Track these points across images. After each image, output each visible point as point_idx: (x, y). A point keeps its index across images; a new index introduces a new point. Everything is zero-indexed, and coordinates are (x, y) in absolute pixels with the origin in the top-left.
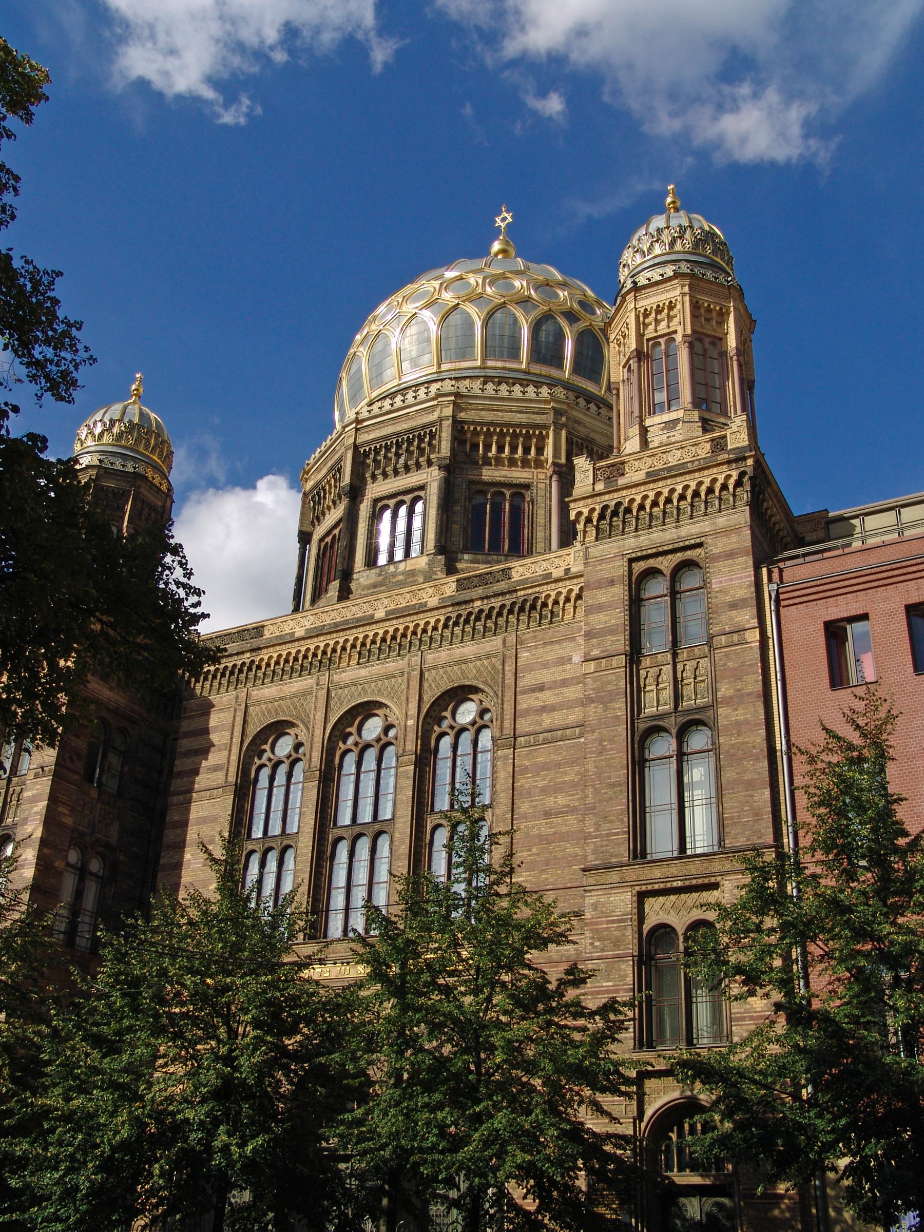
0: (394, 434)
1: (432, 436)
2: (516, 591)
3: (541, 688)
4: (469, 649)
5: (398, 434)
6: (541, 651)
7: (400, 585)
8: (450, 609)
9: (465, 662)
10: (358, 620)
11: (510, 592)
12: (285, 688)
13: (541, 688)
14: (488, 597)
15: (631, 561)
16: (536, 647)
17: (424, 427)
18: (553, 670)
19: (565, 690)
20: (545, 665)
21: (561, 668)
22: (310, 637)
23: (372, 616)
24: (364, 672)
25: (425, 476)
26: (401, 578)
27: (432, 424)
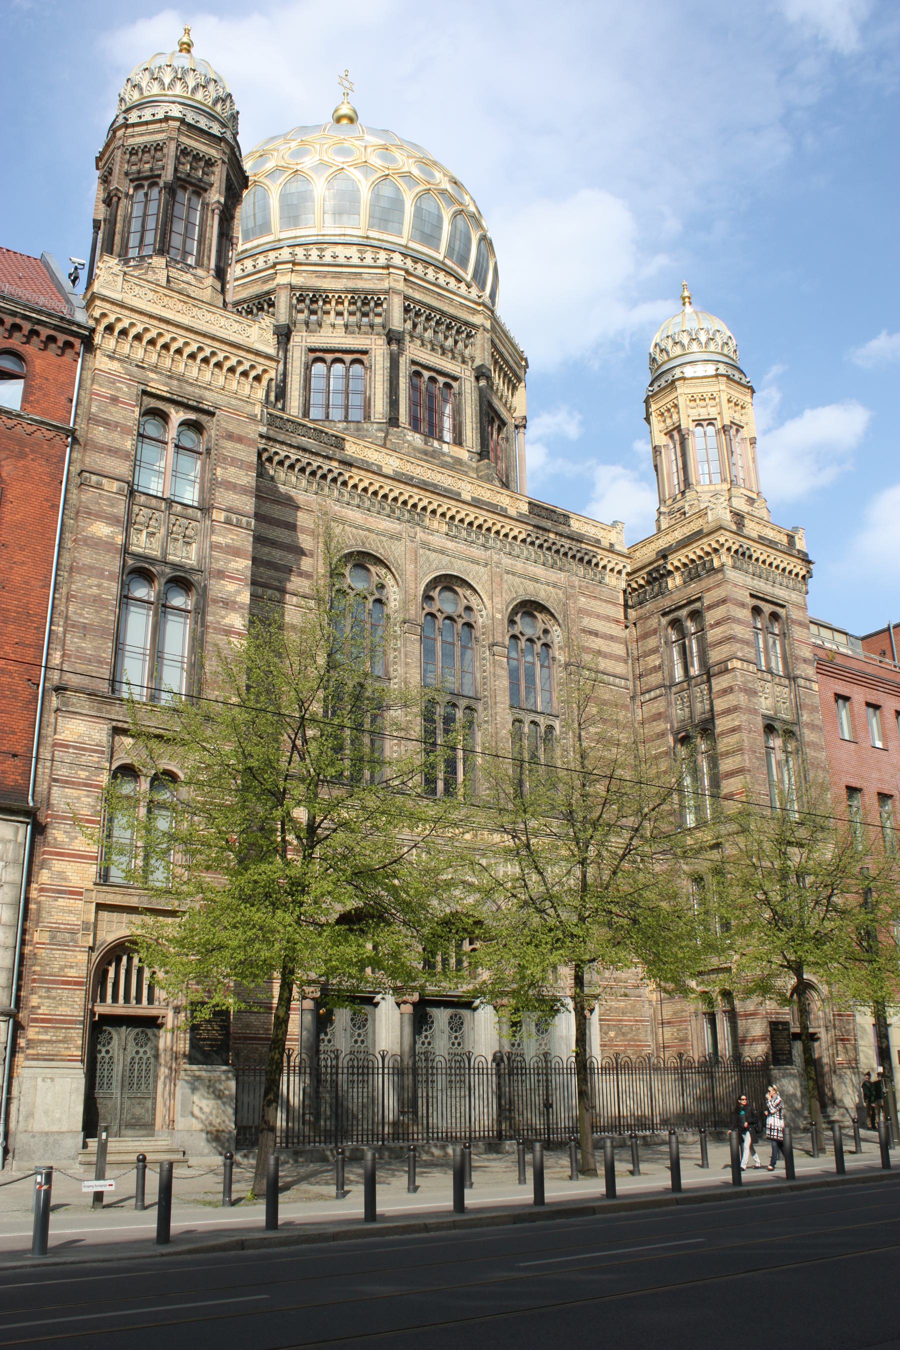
0: (440, 310)
1: (469, 336)
2: (581, 542)
3: (596, 634)
4: (539, 571)
5: (443, 313)
6: (593, 602)
7: (444, 465)
8: (530, 528)
9: (537, 581)
10: (446, 490)
11: (578, 541)
12: (370, 519)
13: (596, 634)
14: (561, 535)
15: (752, 596)
16: (590, 597)
17: (467, 323)
18: (603, 623)
19: (612, 644)
20: (598, 616)
21: (609, 625)
22: (399, 481)
23: (459, 494)
24: (450, 545)
25: (458, 369)
26: (449, 459)
27: (474, 326)
